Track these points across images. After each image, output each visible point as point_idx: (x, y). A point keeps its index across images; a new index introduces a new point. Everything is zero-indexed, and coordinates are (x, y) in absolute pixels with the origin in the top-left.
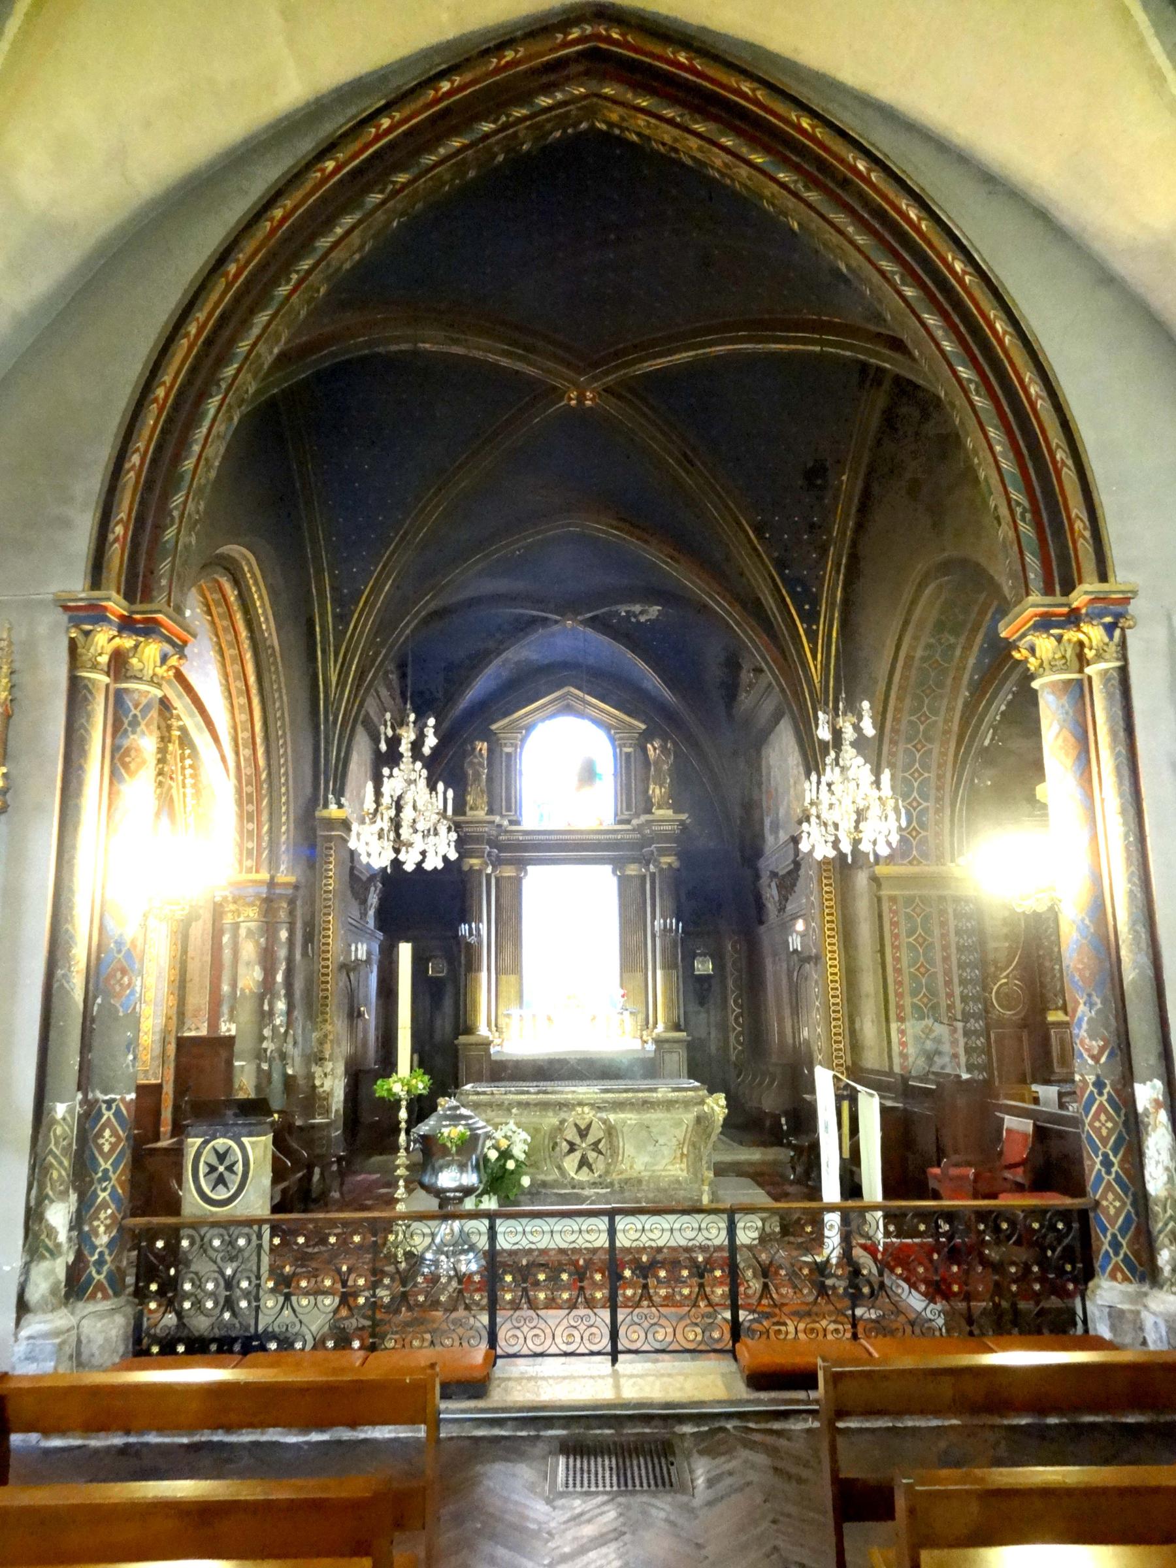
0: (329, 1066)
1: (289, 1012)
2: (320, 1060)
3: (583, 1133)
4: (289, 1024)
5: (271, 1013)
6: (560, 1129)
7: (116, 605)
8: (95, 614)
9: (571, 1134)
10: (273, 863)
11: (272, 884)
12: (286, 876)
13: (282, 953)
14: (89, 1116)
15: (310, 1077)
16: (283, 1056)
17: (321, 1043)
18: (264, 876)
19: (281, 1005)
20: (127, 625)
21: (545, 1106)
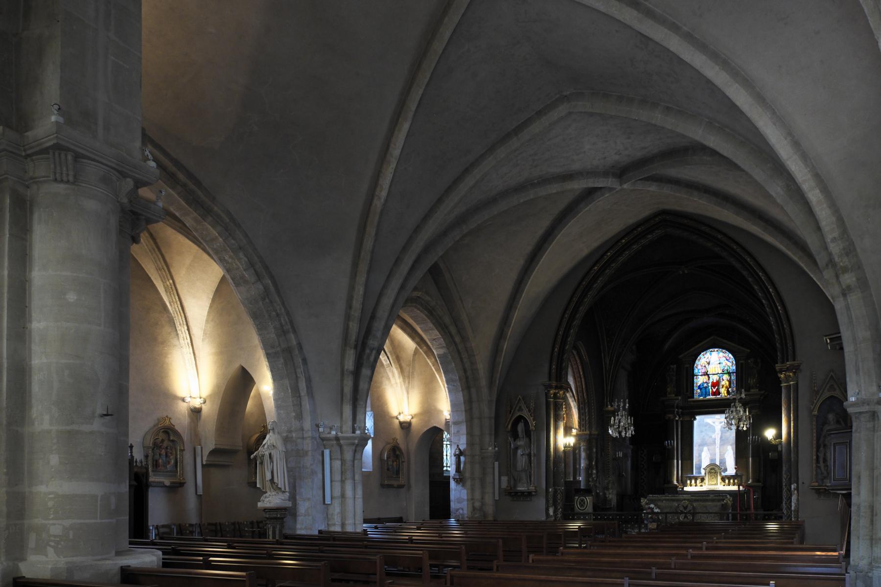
0: (611, 491)
1: (597, 472)
2: (608, 489)
3: (685, 508)
4: (597, 477)
5: (592, 474)
6: (678, 507)
7: (554, 384)
8: (548, 387)
9: (681, 509)
10: (590, 428)
11: (590, 434)
12: (595, 432)
13: (594, 455)
14: (555, 492)
15: (605, 494)
16: (596, 487)
17: (608, 484)
18: (588, 432)
19: (594, 472)
20: (556, 388)
21: (673, 500)
